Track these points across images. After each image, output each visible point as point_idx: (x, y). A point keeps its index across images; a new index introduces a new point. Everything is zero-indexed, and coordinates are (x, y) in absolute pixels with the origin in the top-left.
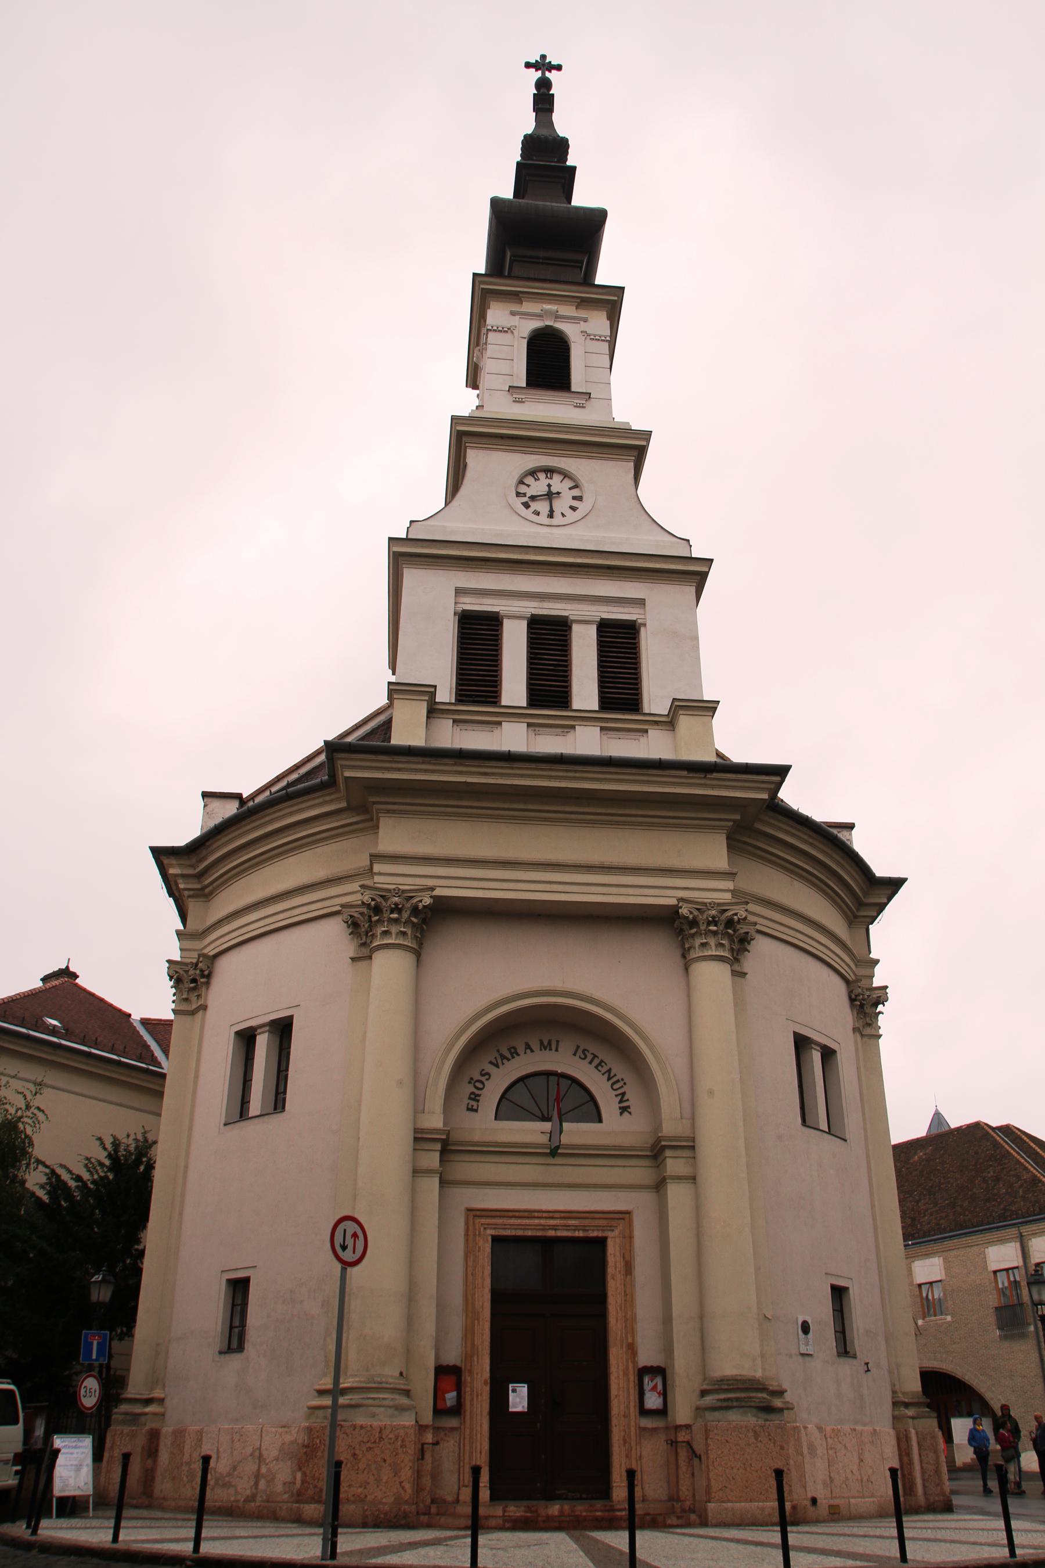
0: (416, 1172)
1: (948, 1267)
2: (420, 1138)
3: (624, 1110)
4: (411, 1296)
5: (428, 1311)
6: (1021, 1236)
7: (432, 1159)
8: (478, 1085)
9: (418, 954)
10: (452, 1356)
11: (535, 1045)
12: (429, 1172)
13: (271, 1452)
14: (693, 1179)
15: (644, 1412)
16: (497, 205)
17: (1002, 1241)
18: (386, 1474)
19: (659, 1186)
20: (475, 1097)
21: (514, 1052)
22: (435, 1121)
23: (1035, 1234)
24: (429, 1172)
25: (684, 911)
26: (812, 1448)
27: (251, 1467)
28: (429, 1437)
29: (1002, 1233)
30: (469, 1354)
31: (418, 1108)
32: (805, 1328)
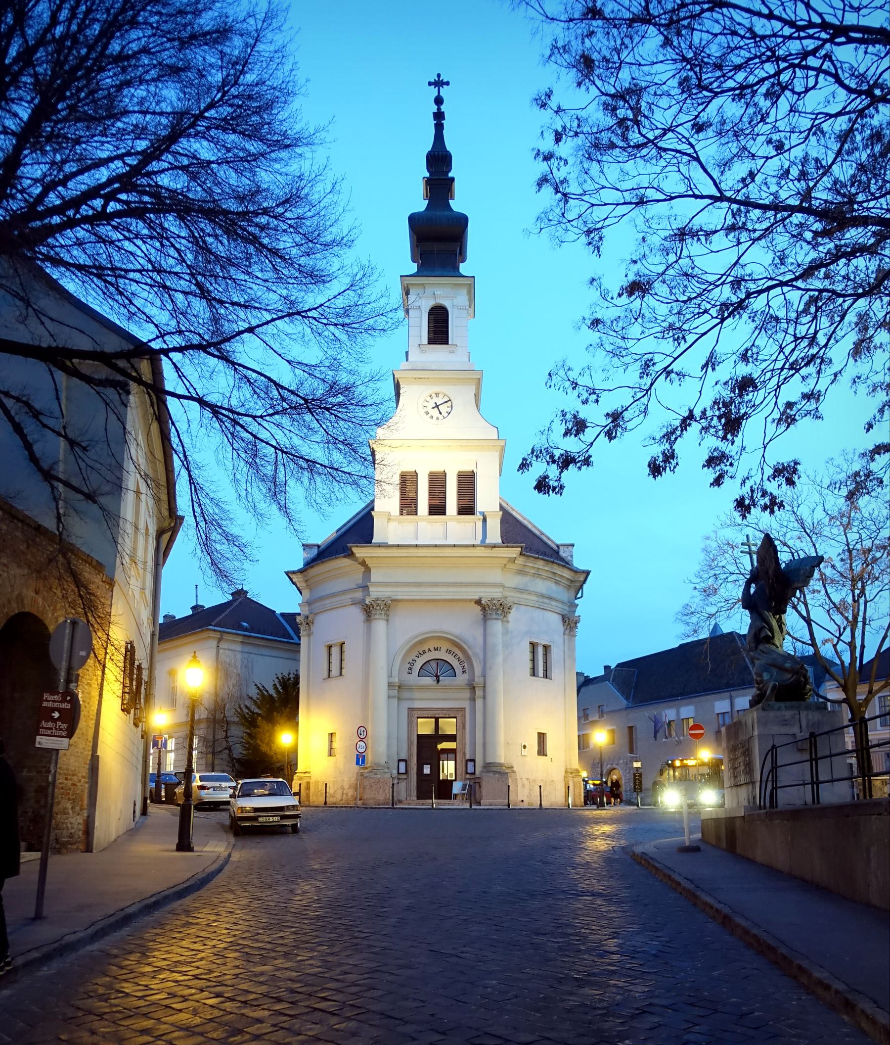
0: (389, 697)
1: (696, 711)
2: (390, 686)
3: (464, 672)
4: (389, 738)
5: (395, 742)
6: (731, 697)
7: (395, 692)
8: (412, 664)
9: (387, 620)
10: (403, 756)
11: (432, 649)
12: (394, 697)
13: (346, 786)
14: (484, 697)
15: (467, 773)
16: (414, 220)
17: (722, 699)
18: (381, 791)
19: (473, 699)
20: (410, 669)
21: (424, 652)
22: (396, 680)
23: (738, 696)
24: (394, 697)
25: (483, 602)
26: (523, 785)
27: (340, 791)
28: (396, 781)
29: (744, 691)
30: (410, 755)
31: (390, 676)
32: (525, 747)
